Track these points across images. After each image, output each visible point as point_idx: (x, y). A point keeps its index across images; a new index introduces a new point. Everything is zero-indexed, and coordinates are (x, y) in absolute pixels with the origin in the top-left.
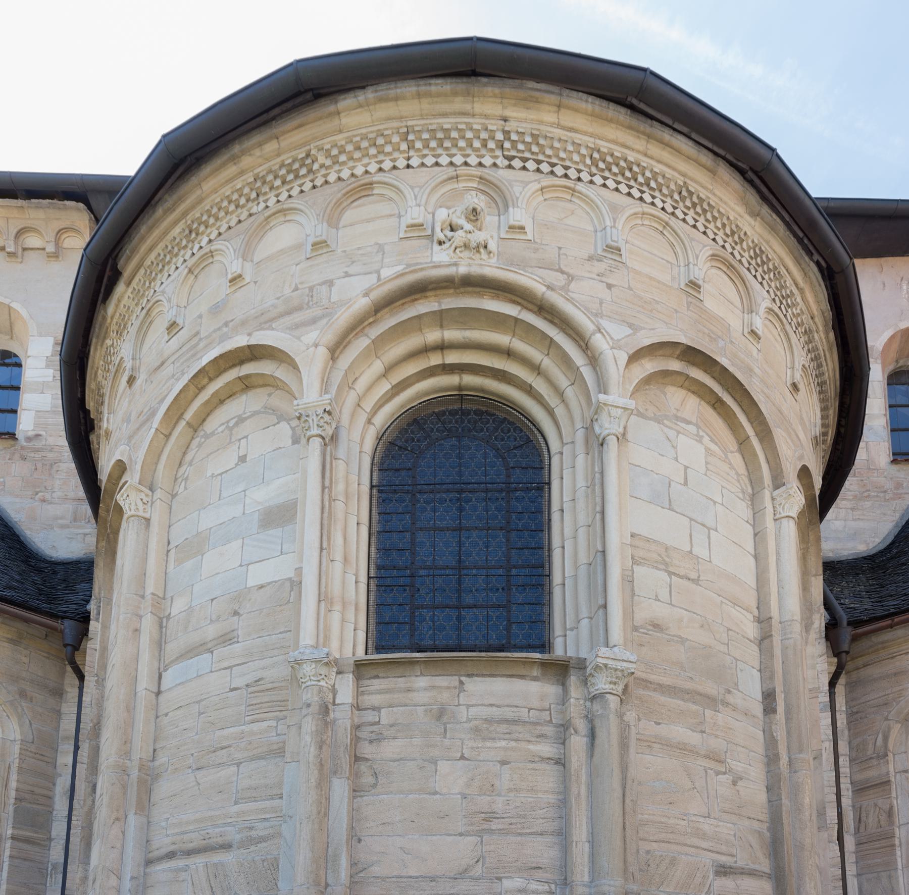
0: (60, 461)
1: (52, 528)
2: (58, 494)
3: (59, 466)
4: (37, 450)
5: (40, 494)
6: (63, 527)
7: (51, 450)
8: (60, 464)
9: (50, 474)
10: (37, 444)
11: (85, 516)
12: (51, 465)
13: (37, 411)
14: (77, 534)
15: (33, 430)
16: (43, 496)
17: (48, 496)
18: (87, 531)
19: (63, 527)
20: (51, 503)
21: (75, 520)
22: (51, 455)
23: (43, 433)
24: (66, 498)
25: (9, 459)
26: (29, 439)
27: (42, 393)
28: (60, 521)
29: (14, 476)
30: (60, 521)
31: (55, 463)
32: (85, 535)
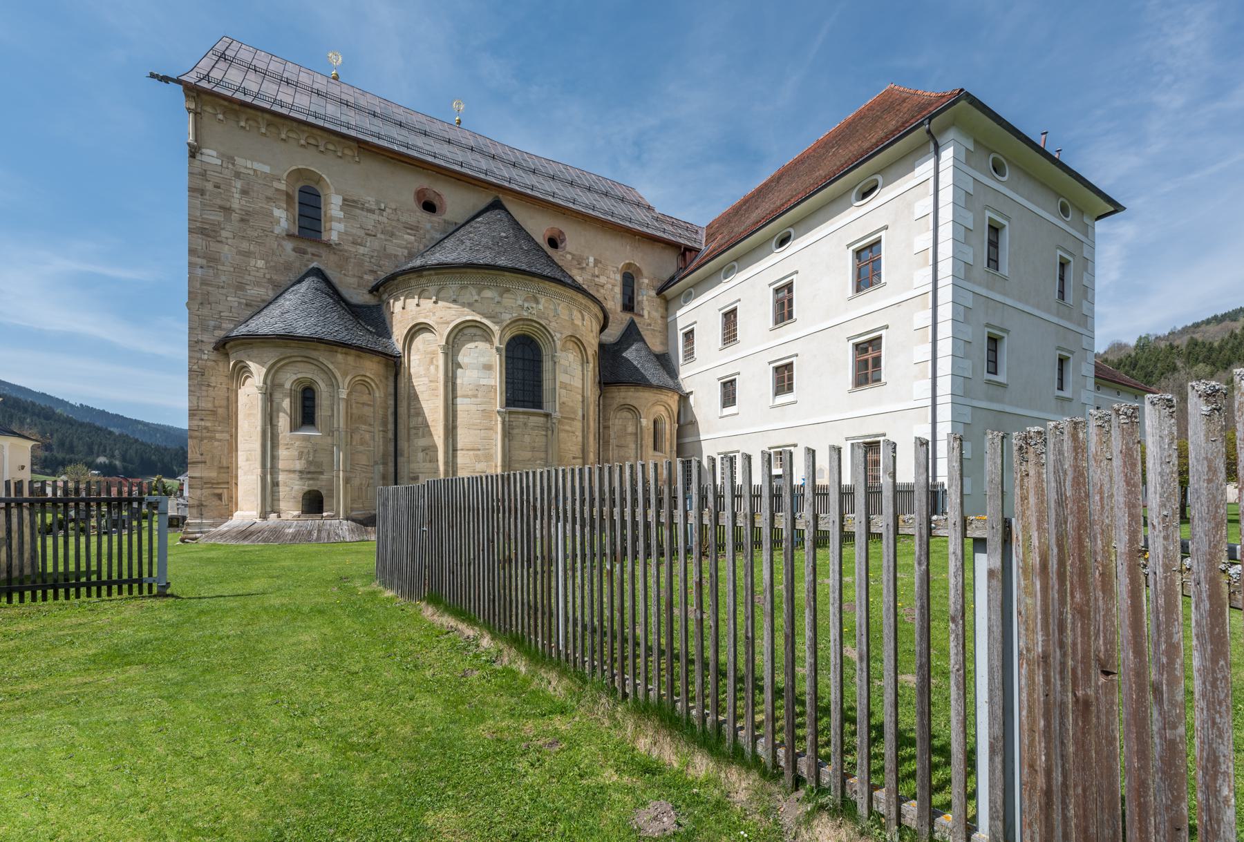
2: (350, 273)
4: (341, 251)
6: (354, 288)
7: (346, 252)
10: (341, 248)
19: (354, 288)
21: (359, 286)
22: (346, 254)
26: (336, 244)
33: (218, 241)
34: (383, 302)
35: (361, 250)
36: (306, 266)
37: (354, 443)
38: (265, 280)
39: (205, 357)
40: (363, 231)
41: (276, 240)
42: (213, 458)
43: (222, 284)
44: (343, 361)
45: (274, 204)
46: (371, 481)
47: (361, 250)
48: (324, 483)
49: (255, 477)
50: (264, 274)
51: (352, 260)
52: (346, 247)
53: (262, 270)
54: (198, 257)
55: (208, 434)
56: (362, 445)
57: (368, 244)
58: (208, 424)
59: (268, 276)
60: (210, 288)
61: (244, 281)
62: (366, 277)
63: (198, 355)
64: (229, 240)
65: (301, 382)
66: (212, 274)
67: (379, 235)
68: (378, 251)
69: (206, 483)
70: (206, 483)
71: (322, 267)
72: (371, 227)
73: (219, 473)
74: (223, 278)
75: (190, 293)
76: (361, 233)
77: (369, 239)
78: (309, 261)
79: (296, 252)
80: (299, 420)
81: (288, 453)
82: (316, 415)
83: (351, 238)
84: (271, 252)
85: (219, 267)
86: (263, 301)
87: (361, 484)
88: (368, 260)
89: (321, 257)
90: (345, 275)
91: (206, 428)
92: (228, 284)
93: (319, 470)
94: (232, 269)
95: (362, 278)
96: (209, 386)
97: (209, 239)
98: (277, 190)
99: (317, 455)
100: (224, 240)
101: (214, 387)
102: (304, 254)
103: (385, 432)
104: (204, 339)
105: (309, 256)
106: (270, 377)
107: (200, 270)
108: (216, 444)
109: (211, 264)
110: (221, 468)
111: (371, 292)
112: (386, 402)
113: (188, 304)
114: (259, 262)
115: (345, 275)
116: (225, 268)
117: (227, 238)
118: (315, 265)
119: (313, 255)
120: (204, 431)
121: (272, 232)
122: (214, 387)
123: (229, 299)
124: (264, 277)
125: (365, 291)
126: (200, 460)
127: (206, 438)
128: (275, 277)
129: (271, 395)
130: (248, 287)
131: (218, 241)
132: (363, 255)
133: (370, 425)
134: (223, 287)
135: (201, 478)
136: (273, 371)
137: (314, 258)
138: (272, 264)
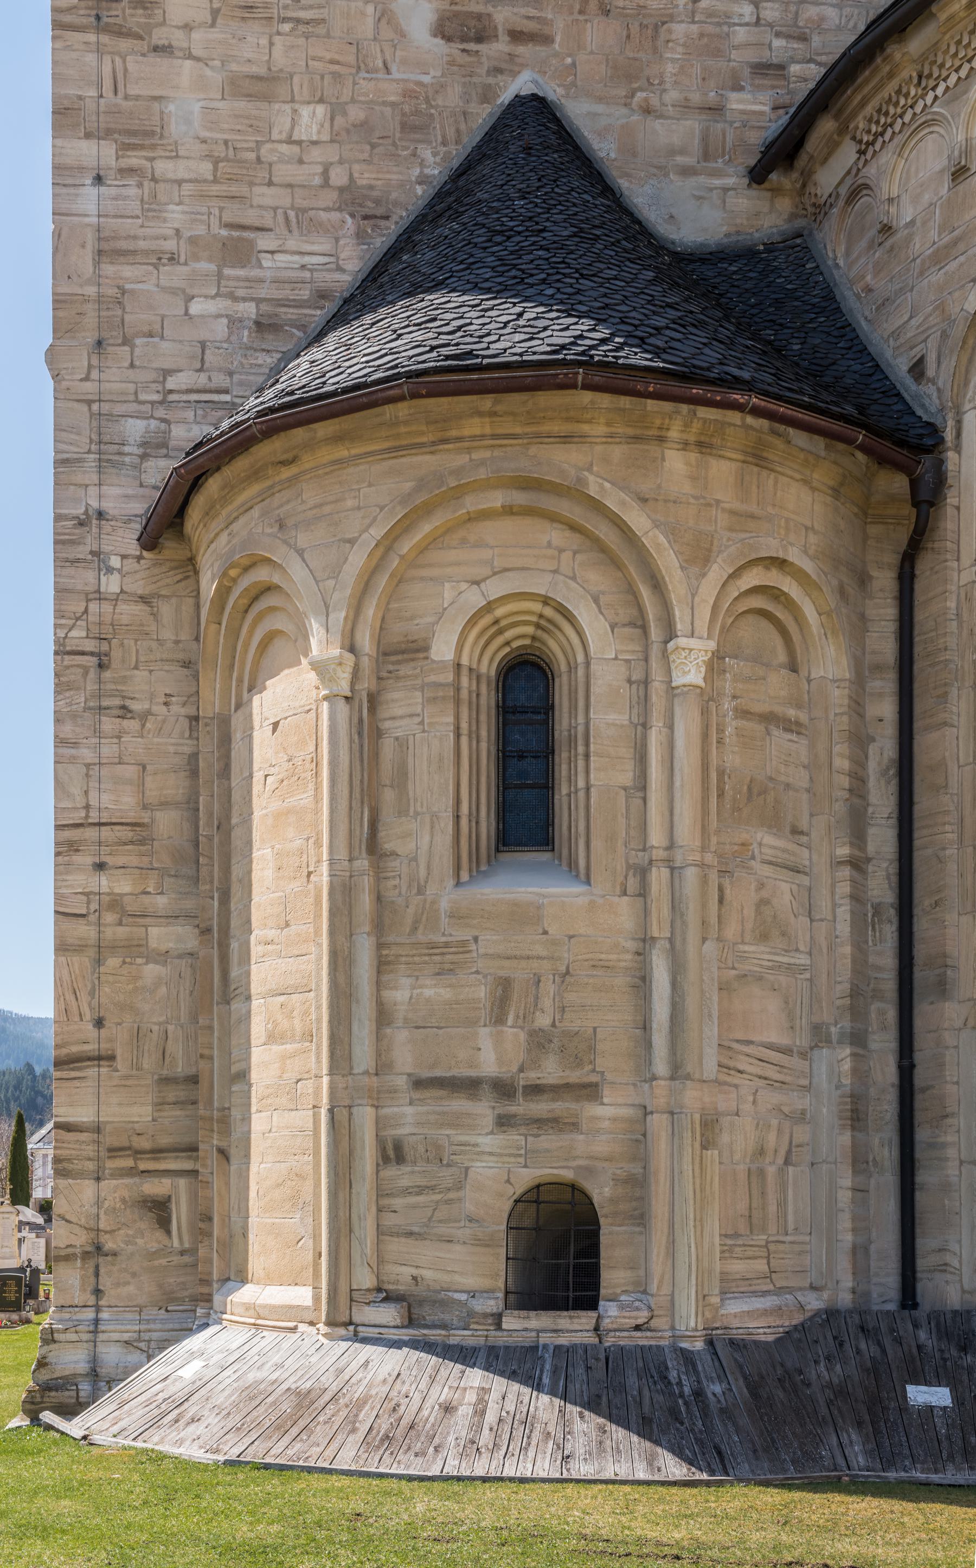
0: (671, 18)
1: (666, 175)
2: (673, 95)
5: (640, 95)
6: (686, 172)
9: (655, 50)
12: (656, 28)
14: (711, 190)
17: (655, 101)
18: (730, 181)
20: (661, 116)
21: (706, 156)
24: (685, 107)
28: (679, 159)
29: (592, 53)
30: (679, 159)
31: (664, 23)
32: (726, 190)
33: (156, 49)
34: (820, 210)
36: (487, 95)
37: (731, 932)
38: (330, 197)
39: (112, 585)
42: (138, 1035)
43: (170, 245)
44: (687, 488)
46: (802, 1134)
48: (602, 1146)
49: (303, 1118)
50: (325, 174)
51: (680, 30)
53: (316, 154)
54: (88, 136)
55: (122, 931)
56: (764, 937)
58: (123, 886)
59: (338, 177)
60: (128, 271)
61: (251, 217)
62: (738, 102)
63: (85, 578)
64: (196, 35)
65: (498, 628)
66: (134, 207)
69: (114, 1151)
70: (114, 1151)
71: (553, 91)
73: (159, 1105)
74: (176, 215)
75: (59, 302)
78: (498, 71)
79: (448, 39)
80: (487, 826)
81: (446, 994)
82: (563, 789)
84: (351, 59)
85: (163, 167)
86: (322, 295)
87: (761, 1152)
89: (546, 40)
90: (647, 110)
91: (115, 903)
92: (193, 241)
93: (574, 1077)
94: (206, 169)
95: (716, 110)
96: (125, 712)
97: (125, 44)
99: (571, 997)
100: (178, 38)
101: (144, 717)
102: (479, 39)
103: (858, 864)
104: (109, 506)
105: (500, 47)
106: (370, 612)
107: (91, 192)
108: (151, 971)
109: (134, 161)
110: (165, 1081)
111: (757, 175)
112: (857, 706)
113: (52, 356)
114: (305, 111)
115: (647, 110)
116: (179, 170)
117: (188, 27)
119: (517, 36)
120: (109, 918)
122: (144, 717)
123: (196, 308)
124: (326, 184)
125: (734, 178)
126: (90, 1048)
127: (113, 948)
128: (365, 176)
129: (373, 701)
130: (264, 242)
131: (156, 49)
133: (796, 831)
134: (173, 259)
135: (97, 1129)
136: (382, 581)
138: (356, 114)
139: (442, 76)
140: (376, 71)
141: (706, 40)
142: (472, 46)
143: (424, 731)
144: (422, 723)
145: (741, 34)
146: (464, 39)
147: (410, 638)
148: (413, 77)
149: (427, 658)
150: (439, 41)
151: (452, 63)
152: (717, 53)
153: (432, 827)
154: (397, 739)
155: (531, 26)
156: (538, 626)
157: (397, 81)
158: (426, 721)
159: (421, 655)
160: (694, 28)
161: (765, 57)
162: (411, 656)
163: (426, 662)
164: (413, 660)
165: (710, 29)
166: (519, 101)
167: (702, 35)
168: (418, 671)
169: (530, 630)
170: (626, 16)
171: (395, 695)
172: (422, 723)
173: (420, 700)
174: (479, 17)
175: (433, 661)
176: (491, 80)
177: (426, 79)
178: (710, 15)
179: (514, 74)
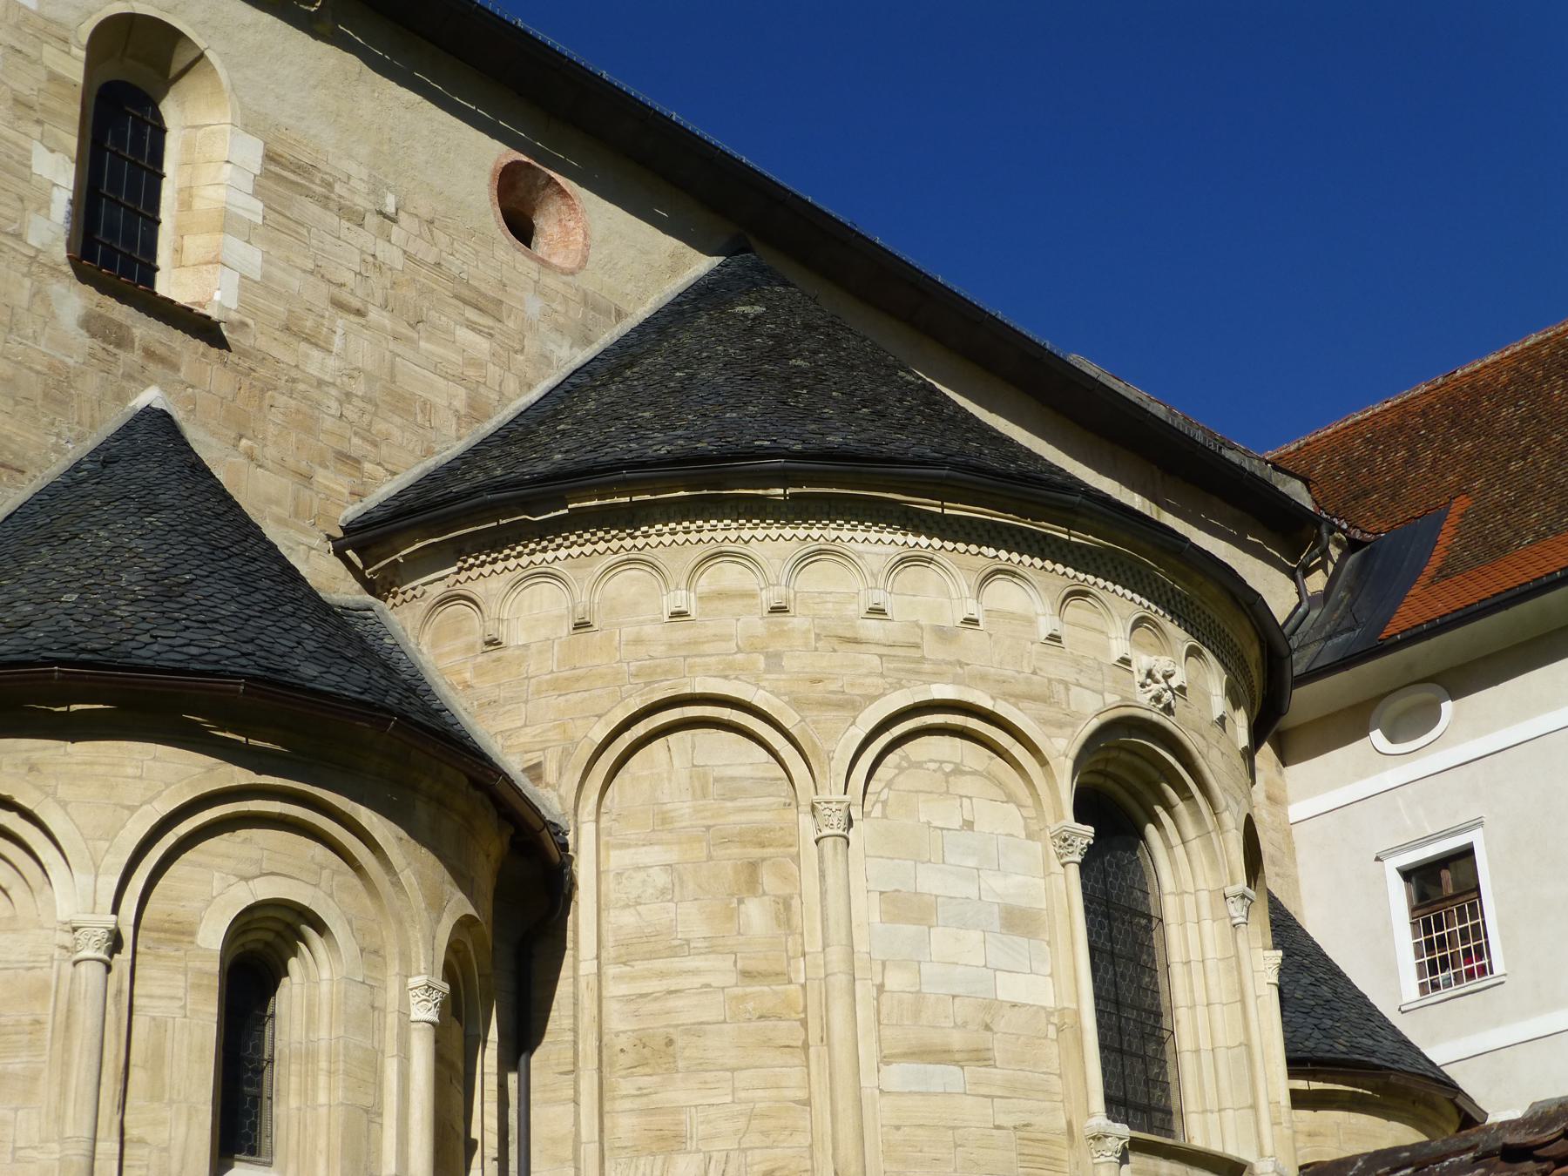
3: (272, 397)
8: (276, 394)
9: (260, 409)
11: (310, 511)
12: (263, 391)
13: (243, 276)
15: (236, 311)
16: (251, 448)
23: (250, 322)
25: (203, 354)
27: (248, 242)
29: (209, 392)
31: (268, 390)
35: (317, 364)
36: (121, 397)
40: (324, 287)
41: (29, 274)
45: (36, 131)
47: (317, 364)
52: (263, 343)
57: (337, 343)
67: (374, 314)
68: (371, 378)
71: (178, 415)
72: (348, 277)
76: (317, 295)
77: (342, 322)
78: (129, 377)
79: (93, 336)
83: (280, 308)
88: (334, 407)
89: (175, 368)
98: (54, 77)
102: (118, 345)
105: (134, 357)
118: (149, 397)
121: (18, 236)
132: (321, 383)
137: (151, 367)
139: (84, 363)
140: (27, 338)
141: (301, 417)
142: (111, 348)
143: (185, 1017)
144: (184, 1007)
145: (328, 423)
146: (105, 339)
147: (173, 918)
148: (58, 355)
149: (192, 943)
150: (83, 332)
151: (92, 355)
152: (309, 431)
153: (189, 1119)
154: (154, 1018)
155: (160, 350)
156: (278, 934)
157: (45, 354)
158: (188, 1007)
159: (187, 939)
160: (293, 402)
161: (344, 448)
162: (175, 937)
163: (191, 947)
164: (177, 941)
165: (304, 407)
166: (148, 411)
167: (298, 411)
168: (181, 953)
169: (269, 937)
170: (238, 372)
171: (154, 973)
172: (184, 1007)
173: (183, 984)
174: (120, 326)
175: (199, 947)
176: (124, 383)
177: (70, 362)
178: (304, 398)
179: (146, 386)
